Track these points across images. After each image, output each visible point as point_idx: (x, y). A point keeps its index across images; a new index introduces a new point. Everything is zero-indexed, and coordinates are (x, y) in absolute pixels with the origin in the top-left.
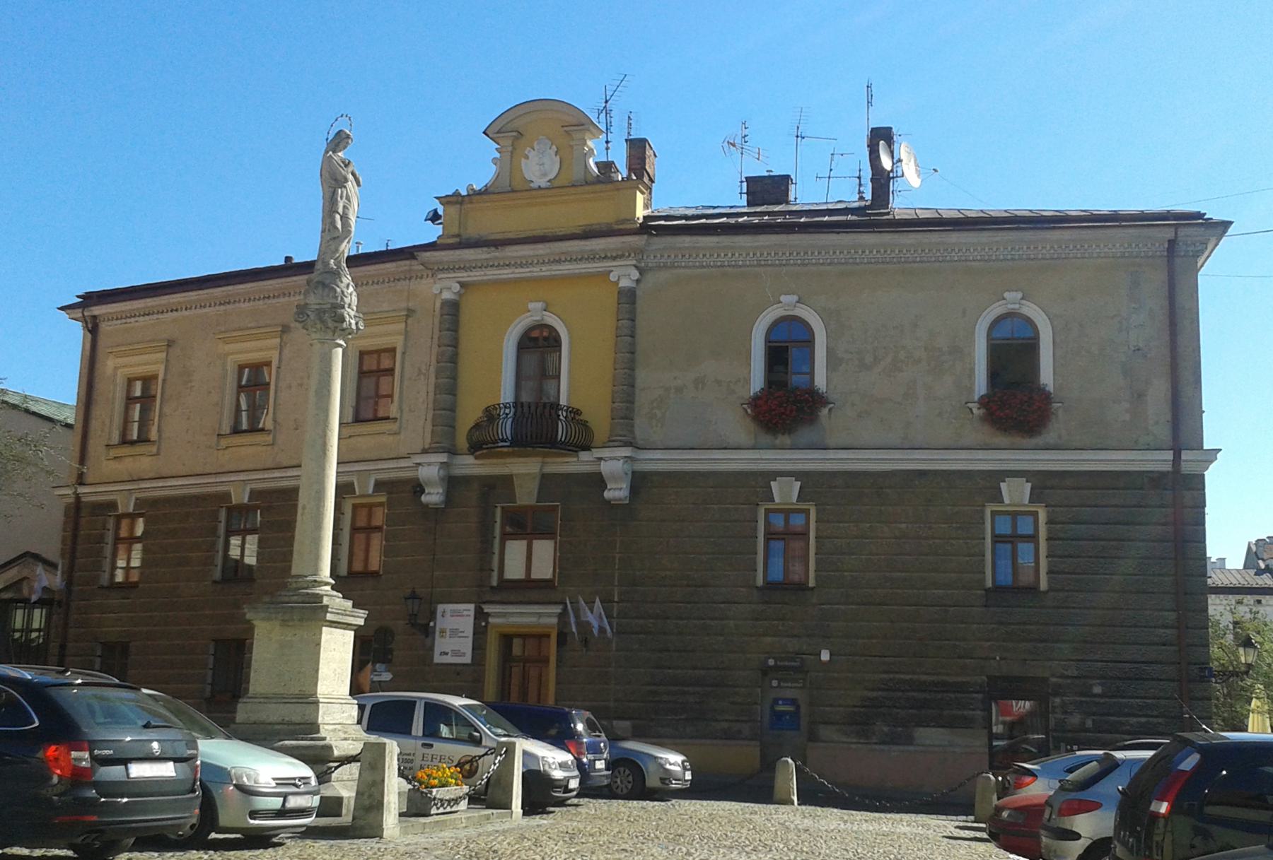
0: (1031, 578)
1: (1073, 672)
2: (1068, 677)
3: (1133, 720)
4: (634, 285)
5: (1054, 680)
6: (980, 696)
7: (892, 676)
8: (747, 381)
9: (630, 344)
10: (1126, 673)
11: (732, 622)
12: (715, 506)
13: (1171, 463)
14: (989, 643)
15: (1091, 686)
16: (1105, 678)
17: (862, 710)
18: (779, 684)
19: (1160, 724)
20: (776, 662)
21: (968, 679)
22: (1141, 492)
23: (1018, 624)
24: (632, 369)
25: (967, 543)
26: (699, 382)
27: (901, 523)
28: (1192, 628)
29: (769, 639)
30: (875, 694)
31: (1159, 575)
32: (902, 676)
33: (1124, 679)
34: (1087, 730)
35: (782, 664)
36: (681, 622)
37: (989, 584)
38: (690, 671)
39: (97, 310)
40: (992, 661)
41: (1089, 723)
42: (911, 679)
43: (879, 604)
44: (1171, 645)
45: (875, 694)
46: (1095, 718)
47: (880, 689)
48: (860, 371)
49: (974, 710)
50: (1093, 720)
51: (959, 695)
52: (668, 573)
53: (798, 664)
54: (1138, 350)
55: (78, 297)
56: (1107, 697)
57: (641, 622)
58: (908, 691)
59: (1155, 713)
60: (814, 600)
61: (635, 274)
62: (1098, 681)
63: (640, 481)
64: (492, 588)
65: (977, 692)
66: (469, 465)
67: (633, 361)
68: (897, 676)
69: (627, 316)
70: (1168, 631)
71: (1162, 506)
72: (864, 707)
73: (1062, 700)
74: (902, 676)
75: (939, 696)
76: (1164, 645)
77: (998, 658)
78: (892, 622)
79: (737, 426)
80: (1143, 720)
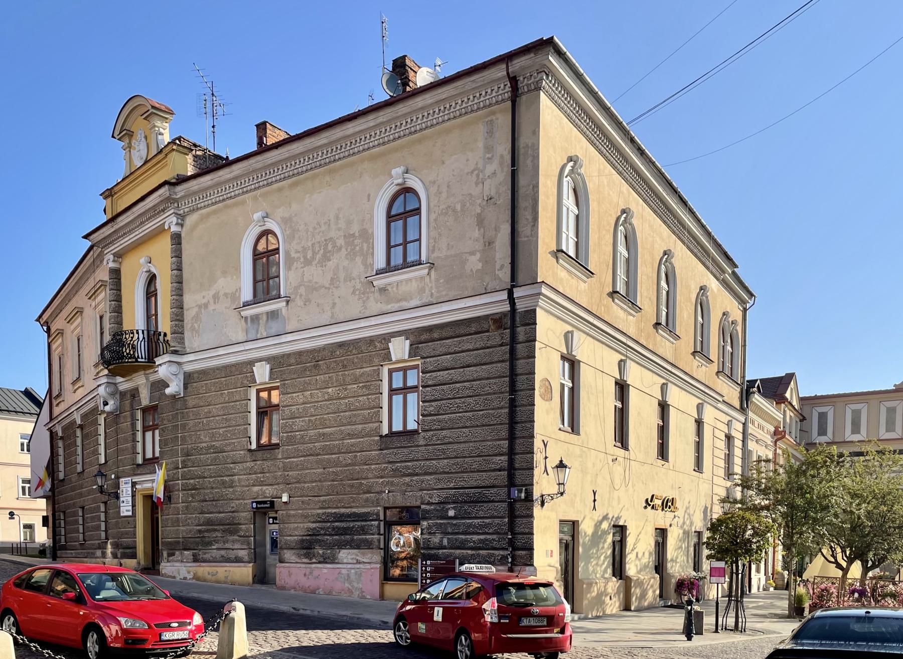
1: (435, 500)
2: (432, 503)
3: (476, 537)
5: (423, 507)
6: (376, 523)
9: (176, 276)
10: (471, 497)
17: (308, 538)
23: (401, 462)
25: (368, 399)
28: (521, 454)
29: (256, 489)
30: (314, 525)
31: (499, 408)
32: (330, 511)
34: (445, 548)
36: (211, 480)
40: (384, 494)
41: (445, 542)
42: (335, 513)
43: (317, 455)
45: (314, 525)
48: (304, 267)
49: (373, 534)
57: (192, 481)
59: (491, 531)
60: (280, 456)
62: (452, 506)
63: (189, 379)
70: (502, 458)
74: (330, 511)
75: (352, 524)
76: (500, 471)
77: (387, 492)
78: (324, 469)
80: (482, 537)
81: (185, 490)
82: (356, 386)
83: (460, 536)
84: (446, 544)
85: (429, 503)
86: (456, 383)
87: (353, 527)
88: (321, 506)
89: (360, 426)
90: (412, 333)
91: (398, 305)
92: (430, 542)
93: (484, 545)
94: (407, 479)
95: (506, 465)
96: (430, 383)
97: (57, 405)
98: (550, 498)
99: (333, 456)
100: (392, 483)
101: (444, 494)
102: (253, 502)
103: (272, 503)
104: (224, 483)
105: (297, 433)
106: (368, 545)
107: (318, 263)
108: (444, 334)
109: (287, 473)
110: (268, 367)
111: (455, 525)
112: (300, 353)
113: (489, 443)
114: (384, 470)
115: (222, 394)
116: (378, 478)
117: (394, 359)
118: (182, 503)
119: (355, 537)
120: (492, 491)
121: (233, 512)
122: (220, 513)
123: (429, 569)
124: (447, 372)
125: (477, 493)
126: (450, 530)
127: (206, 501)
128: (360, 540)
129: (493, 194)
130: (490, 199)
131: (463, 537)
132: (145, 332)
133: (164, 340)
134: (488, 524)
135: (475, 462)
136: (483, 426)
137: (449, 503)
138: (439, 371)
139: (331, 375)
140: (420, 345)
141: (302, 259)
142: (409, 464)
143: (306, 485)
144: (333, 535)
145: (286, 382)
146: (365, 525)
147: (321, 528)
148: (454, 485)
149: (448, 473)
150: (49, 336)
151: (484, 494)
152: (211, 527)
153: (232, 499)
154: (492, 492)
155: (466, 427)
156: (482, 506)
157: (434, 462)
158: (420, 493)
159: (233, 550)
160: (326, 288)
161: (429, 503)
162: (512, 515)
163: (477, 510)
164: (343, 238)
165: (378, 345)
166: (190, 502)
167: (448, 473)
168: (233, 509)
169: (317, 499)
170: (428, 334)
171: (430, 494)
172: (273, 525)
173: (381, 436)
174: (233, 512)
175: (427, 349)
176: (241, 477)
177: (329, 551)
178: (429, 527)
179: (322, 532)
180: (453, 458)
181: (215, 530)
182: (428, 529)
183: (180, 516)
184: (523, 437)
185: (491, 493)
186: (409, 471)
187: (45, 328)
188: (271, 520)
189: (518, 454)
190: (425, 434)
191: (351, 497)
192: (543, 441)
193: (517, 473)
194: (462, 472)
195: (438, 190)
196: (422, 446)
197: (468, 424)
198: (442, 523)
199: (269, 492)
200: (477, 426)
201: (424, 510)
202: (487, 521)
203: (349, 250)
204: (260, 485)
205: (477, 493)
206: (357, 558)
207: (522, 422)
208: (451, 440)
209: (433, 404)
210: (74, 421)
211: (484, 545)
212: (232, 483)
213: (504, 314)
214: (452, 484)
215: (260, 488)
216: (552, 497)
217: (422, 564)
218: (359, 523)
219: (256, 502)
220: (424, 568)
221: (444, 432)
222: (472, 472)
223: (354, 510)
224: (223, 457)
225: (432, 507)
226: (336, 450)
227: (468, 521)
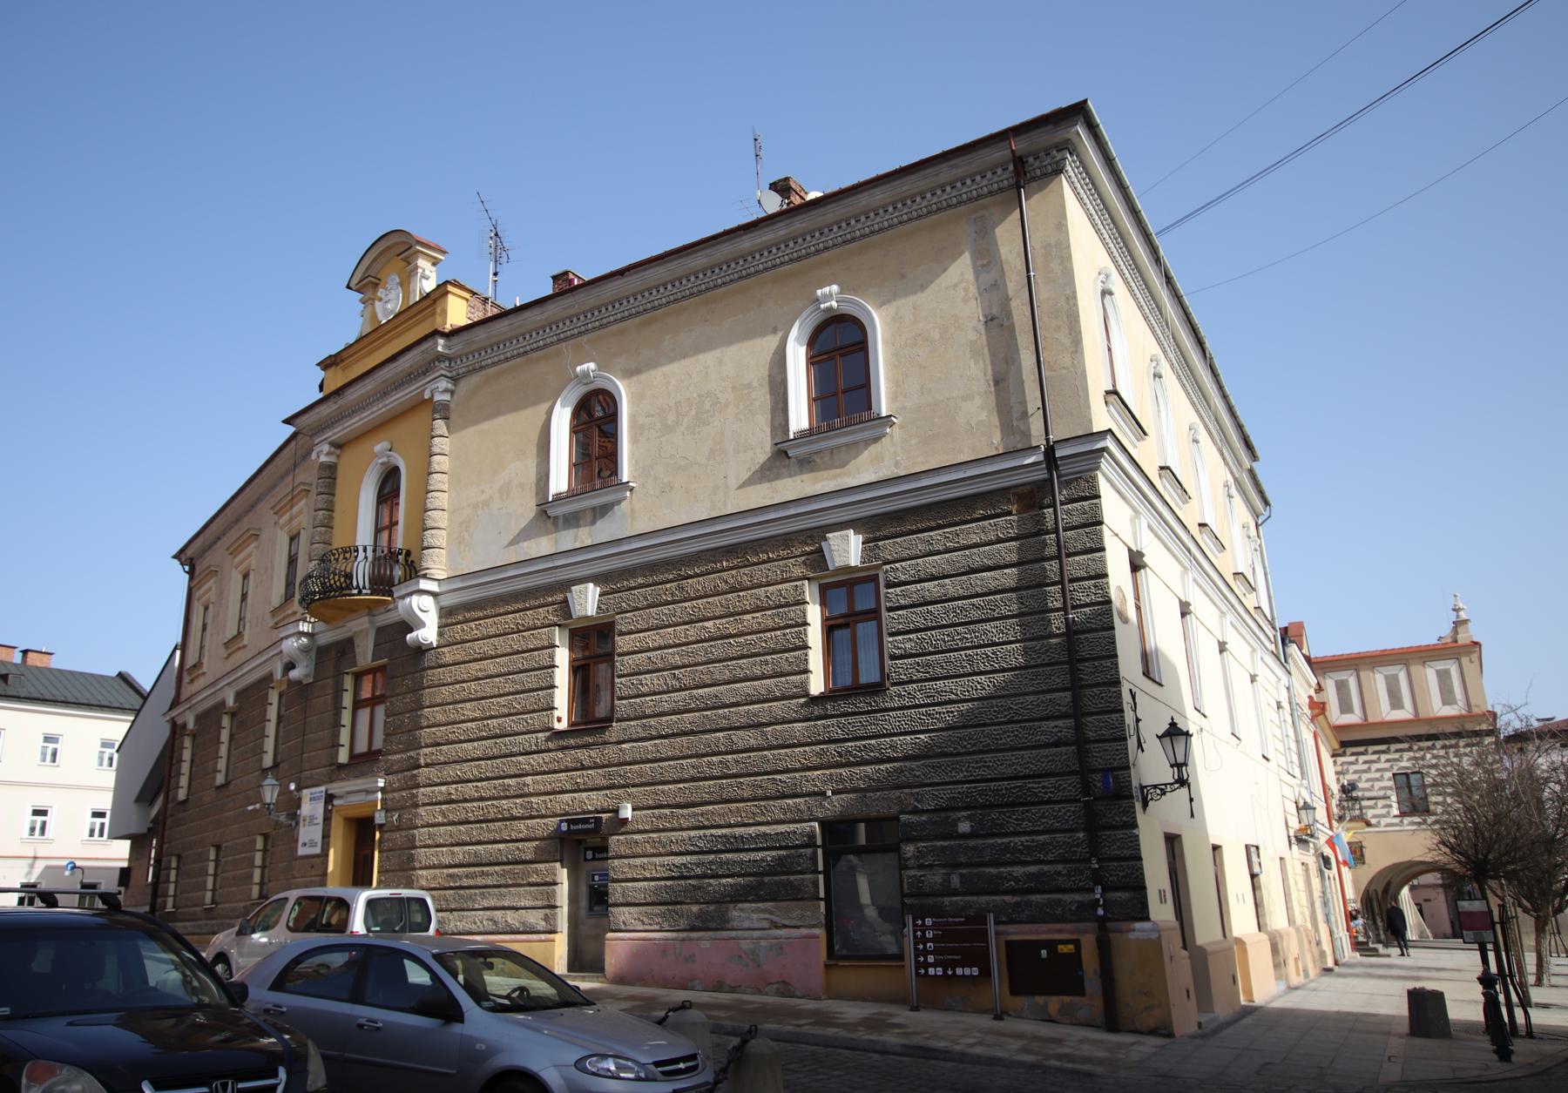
2: (923, 812)
3: (1019, 870)
5: (903, 817)
6: (809, 851)
7: (701, 832)
16: (974, 808)
17: (669, 883)
18: (594, 855)
19: (1059, 873)
20: (569, 826)
33: (1001, 806)
34: (955, 893)
35: (575, 827)
36: (479, 784)
38: (490, 846)
41: (955, 880)
42: (724, 836)
44: (1066, 744)
49: (802, 873)
50: (962, 875)
57: (443, 788)
59: (1050, 857)
61: (444, 384)
62: (964, 814)
68: (708, 832)
70: (1060, 723)
74: (713, 831)
76: (1057, 746)
80: (1033, 869)
83: (987, 870)
84: (958, 885)
85: (916, 811)
86: (955, 599)
91: (835, 482)
92: (923, 882)
95: (1070, 734)
97: (192, 681)
98: (1158, 791)
101: (945, 793)
102: (561, 821)
104: (507, 788)
107: (688, 428)
109: (628, 767)
111: (974, 848)
113: (1029, 698)
120: (1046, 782)
123: (930, 934)
124: (936, 582)
125: (1015, 788)
128: (776, 883)
129: (994, 312)
130: (992, 320)
131: (993, 870)
132: (370, 550)
133: (406, 561)
134: (1043, 844)
135: (1005, 732)
140: (880, 543)
141: (658, 425)
142: (873, 742)
147: (698, 865)
148: (965, 776)
149: (952, 755)
150: (191, 578)
154: (1046, 784)
156: (1027, 811)
157: (922, 736)
158: (897, 793)
159: (517, 909)
160: (701, 465)
161: (916, 811)
162: (1093, 826)
163: (1017, 819)
164: (730, 390)
167: (952, 755)
169: (685, 811)
171: (917, 793)
172: (595, 863)
177: (712, 908)
178: (920, 854)
179: (699, 871)
181: (483, 874)
182: (917, 858)
184: (1098, 685)
185: (1044, 787)
186: (872, 754)
187: (187, 568)
188: (589, 855)
192: (1131, 690)
194: (981, 752)
195: (897, 314)
198: (946, 847)
199: (593, 801)
201: (906, 824)
202: (1041, 838)
203: (741, 407)
205: (1015, 788)
206: (772, 917)
210: (223, 703)
214: (962, 775)
216: (1161, 790)
217: (915, 925)
219: (567, 821)
220: (919, 933)
221: (940, 683)
222: (999, 751)
225: (924, 818)
227: (999, 841)
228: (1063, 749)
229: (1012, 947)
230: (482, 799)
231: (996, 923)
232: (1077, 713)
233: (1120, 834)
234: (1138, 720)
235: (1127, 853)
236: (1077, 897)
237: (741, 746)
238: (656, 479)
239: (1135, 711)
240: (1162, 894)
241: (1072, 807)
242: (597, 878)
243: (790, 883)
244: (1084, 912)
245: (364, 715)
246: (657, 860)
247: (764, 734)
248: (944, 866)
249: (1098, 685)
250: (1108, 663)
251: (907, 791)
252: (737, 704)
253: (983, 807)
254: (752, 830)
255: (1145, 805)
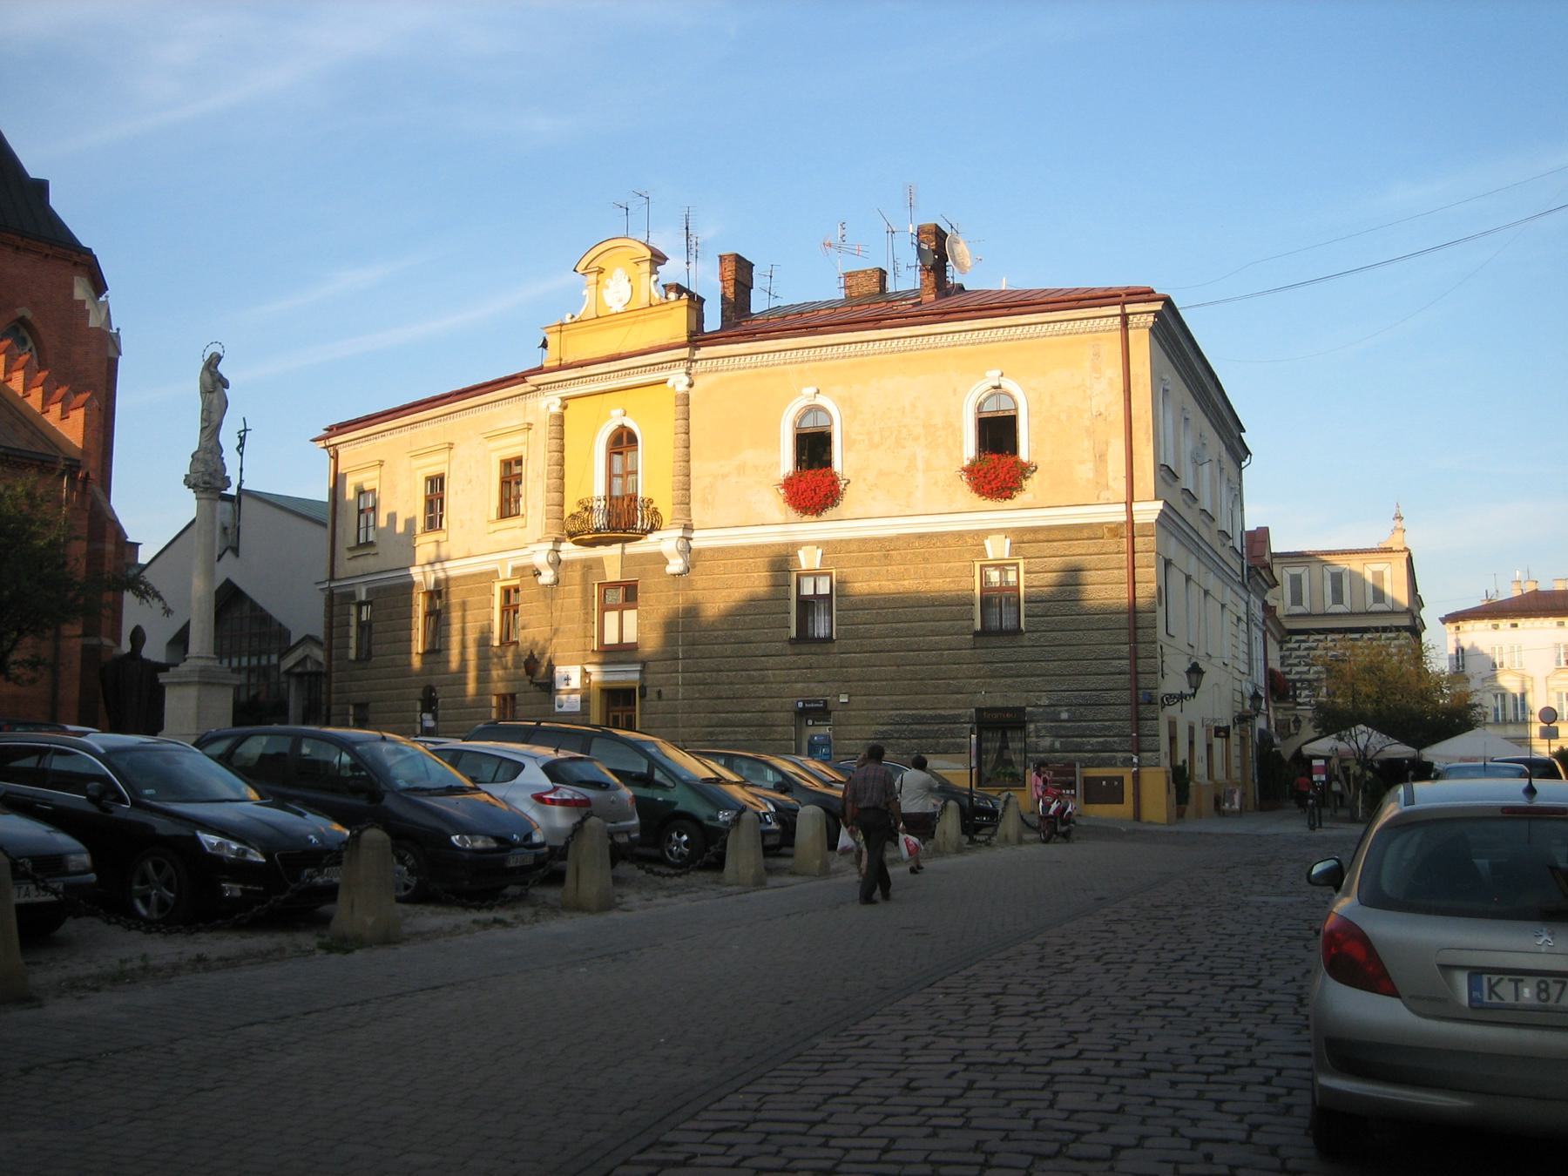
0: (1014, 623)
1: (1045, 701)
2: (1041, 706)
3: (1094, 740)
4: (686, 389)
5: (1029, 709)
6: (970, 726)
7: (898, 712)
8: (778, 464)
11: (770, 672)
12: (755, 575)
13: (1125, 513)
14: (976, 681)
15: (1059, 713)
16: (1070, 705)
18: (813, 722)
19: (1115, 742)
20: (804, 705)
21: (960, 711)
22: (1101, 541)
24: (688, 461)
26: (741, 469)
27: (905, 580)
28: (1145, 658)
29: (800, 685)
30: (885, 728)
32: (907, 712)
33: (1086, 705)
35: (809, 705)
36: (729, 674)
37: (978, 626)
38: (739, 715)
39: (334, 441)
40: (979, 695)
41: (1057, 745)
43: (888, 651)
45: (885, 728)
46: (1062, 740)
47: (891, 724)
49: (964, 738)
50: (1061, 742)
51: (952, 726)
52: (720, 633)
53: (822, 705)
54: (1100, 415)
55: (325, 430)
56: (1073, 721)
57: (700, 675)
58: (912, 724)
59: (1111, 733)
60: (836, 651)
62: (1066, 708)
64: (593, 651)
65: (968, 723)
66: (569, 551)
67: (688, 454)
68: (902, 712)
69: (681, 417)
70: (1123, 662)
71: (1118, 553)
72: (875, 739)
73: (1036, 726)
74: (907, 712)
75: (936, 728)
78: (898, 666)
79: (773, 504)
81: (689, 685)
82: (941, 581)
83: (1075, 739)
87: (938, 731)
88: (895, 707)
89: (948, 623)
90: (1013, 532)
93: (1105, 748)
94: (1009, 681)
96: (1035, 584)
99: (912, 653)
100: (990, 684)
103: (825, 702)
105: (861, 627)
106: (959, 749)
108: (1052, 537)
110: (820, 552)
111: (1068, 728)
112: (865, 541)
113: (1106, 647)
114: (979, 670)
115: (748, 576)
116: (971, 678)
117: (991, 557)
118: (684, 699)
119: (941, 741)
120: (1113, 694)
121: (764, 712)
122: (743, 712)
126: (1063, 733)
127: (722, 698)
131: (1079, 740)
136: (1098, 629)
137: (1061, 705)
138: (1046, 572)
139: (906, 567)
140: (1023, 545)
142: (1012, 665)
143: (873, 684)
144: (910, 738)
145: (845, 570)
146: (954, 728)
147: (897, 732)
149: (1059, 675)
151: (1103, 697)
152: (729, 729)
153: (763, 697)
155: (1080, 630)
157: (1043, 664)
158: (1025, 694)
162: (1137, 719)
165: (970, 541)
166: (696, 698)
167: (1059, 675)
168: (763, 709)
170: (1032, 535)
173: (976, 634)
174: (764, 712)
175: (1031, 549)
176: (777, 672)
177: (905, 756)
178: (1037, 730)
179: (895, 735)
180: (1065, 660)
181: (735, 733)
183: (679, 716)
184: (1145, 643)
188: (810, 722)
189: (1140, 658)
190: (1030, 634)
191: (936, 698)
193: (1141, 676)
196: (1026, 646)
197: (1082, 627)
199: (819, 690)
200: (1093, 629)
201: (1031, 713)
202: (1107, 723)
204: (805, 682)
207: (1143, 628)
208: (1062, 642)
209: (1040, 604)
211: (1105, 748)
212: (763, 679)
213: (1120, 524)
215: (805, 685)
218: (947, 726)
219: (801, 701)
221: (1054, 634)
223: (939, 712)
224: (750, 648)
225: (1041, 710)
226: (915, 647)
227: (1084, 724)
228: (1123, 676)
229: (1088, 781)
230: (731, 683)
231: (1081, 767)
232: (1134, 657)
233: (1149, 723)
234: (1163, 662)
235: (1152, 733)
236: (1125, 755)
237: (926, 660)
238: (865, 480)
239: (1162, 657)
240: (1166, 753)
241: (1125, 708)
242: (816, 738)
243: (958, 744)
244: (1127, 763)
245: (611, 618)
246: (867, 728)
247: (942, 655)
248: (1053, 736)
249: (1145, 643)
250: (1151, 631)
251: (1032, 694)
252: (924, 636)
253: (1075, 705)
254: (931, 712)
255: (1163, 708)
